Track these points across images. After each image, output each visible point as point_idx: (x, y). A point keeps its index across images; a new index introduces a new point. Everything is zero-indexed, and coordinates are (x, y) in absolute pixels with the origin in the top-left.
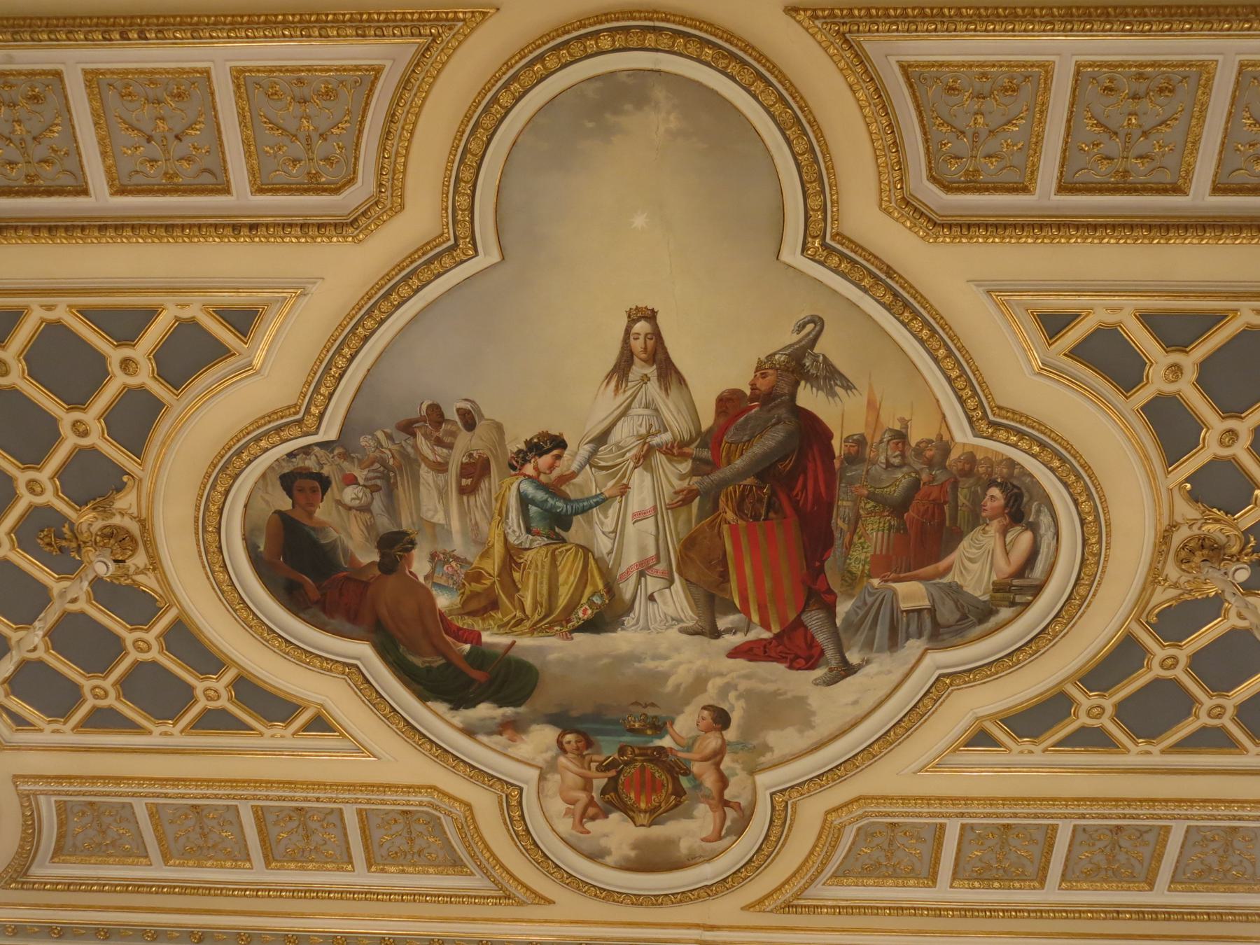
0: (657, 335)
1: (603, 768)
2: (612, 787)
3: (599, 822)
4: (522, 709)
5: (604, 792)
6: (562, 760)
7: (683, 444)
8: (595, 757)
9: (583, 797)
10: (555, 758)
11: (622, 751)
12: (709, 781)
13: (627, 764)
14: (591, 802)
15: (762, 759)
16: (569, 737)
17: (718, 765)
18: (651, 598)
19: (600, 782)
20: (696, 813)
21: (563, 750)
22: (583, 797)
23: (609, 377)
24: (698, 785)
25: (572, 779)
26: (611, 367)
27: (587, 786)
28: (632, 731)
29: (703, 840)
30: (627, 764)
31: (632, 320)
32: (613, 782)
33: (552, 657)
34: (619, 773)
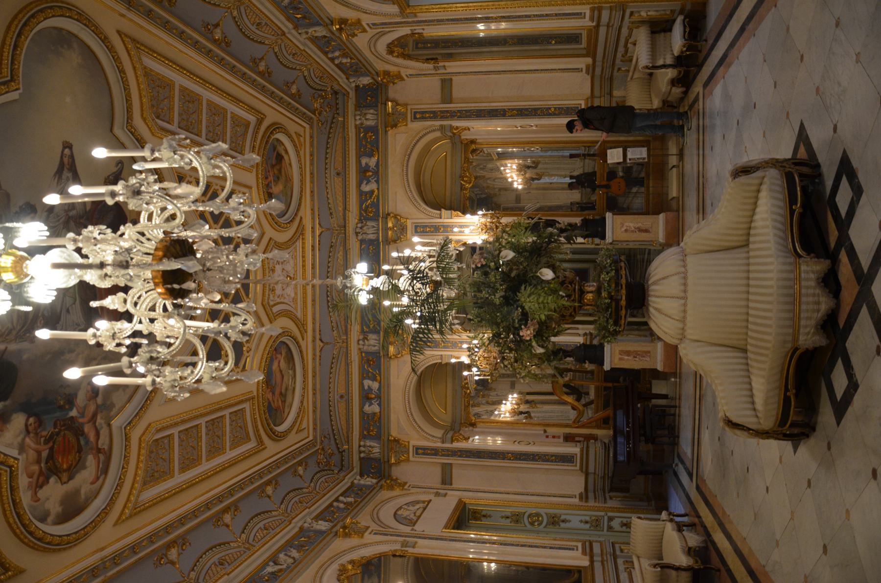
0: (72, 156)
1: (46, 442)
2: (51, 457)
3: (45, 488)
4: (8, 403)
5: (46, 463)
6: (28, 440)
7: (81, 217)
8: (44, 433)
9: (35, 468)
10: (24, 439)
11: (55, 426)
12: (92, 438)
13: (58, 434)
14: (41, 473)
15: (112, 413)
16: (31, 420)
17: (95, 423)
18: (68, 311)
19: (45, 454)
20: (88, 464)
21: (28, 432)
22: (35, 468)
23: (55, 175)
24: (87, 442)
25: (32, 454)
26: (55, 170)
27: (38, 462)
28: (61, 408)
29: (92, 483)
30: (58, 434)
31: (64, 148)
32: (51, 449)
33: (25, 357)
34: (54, 443)
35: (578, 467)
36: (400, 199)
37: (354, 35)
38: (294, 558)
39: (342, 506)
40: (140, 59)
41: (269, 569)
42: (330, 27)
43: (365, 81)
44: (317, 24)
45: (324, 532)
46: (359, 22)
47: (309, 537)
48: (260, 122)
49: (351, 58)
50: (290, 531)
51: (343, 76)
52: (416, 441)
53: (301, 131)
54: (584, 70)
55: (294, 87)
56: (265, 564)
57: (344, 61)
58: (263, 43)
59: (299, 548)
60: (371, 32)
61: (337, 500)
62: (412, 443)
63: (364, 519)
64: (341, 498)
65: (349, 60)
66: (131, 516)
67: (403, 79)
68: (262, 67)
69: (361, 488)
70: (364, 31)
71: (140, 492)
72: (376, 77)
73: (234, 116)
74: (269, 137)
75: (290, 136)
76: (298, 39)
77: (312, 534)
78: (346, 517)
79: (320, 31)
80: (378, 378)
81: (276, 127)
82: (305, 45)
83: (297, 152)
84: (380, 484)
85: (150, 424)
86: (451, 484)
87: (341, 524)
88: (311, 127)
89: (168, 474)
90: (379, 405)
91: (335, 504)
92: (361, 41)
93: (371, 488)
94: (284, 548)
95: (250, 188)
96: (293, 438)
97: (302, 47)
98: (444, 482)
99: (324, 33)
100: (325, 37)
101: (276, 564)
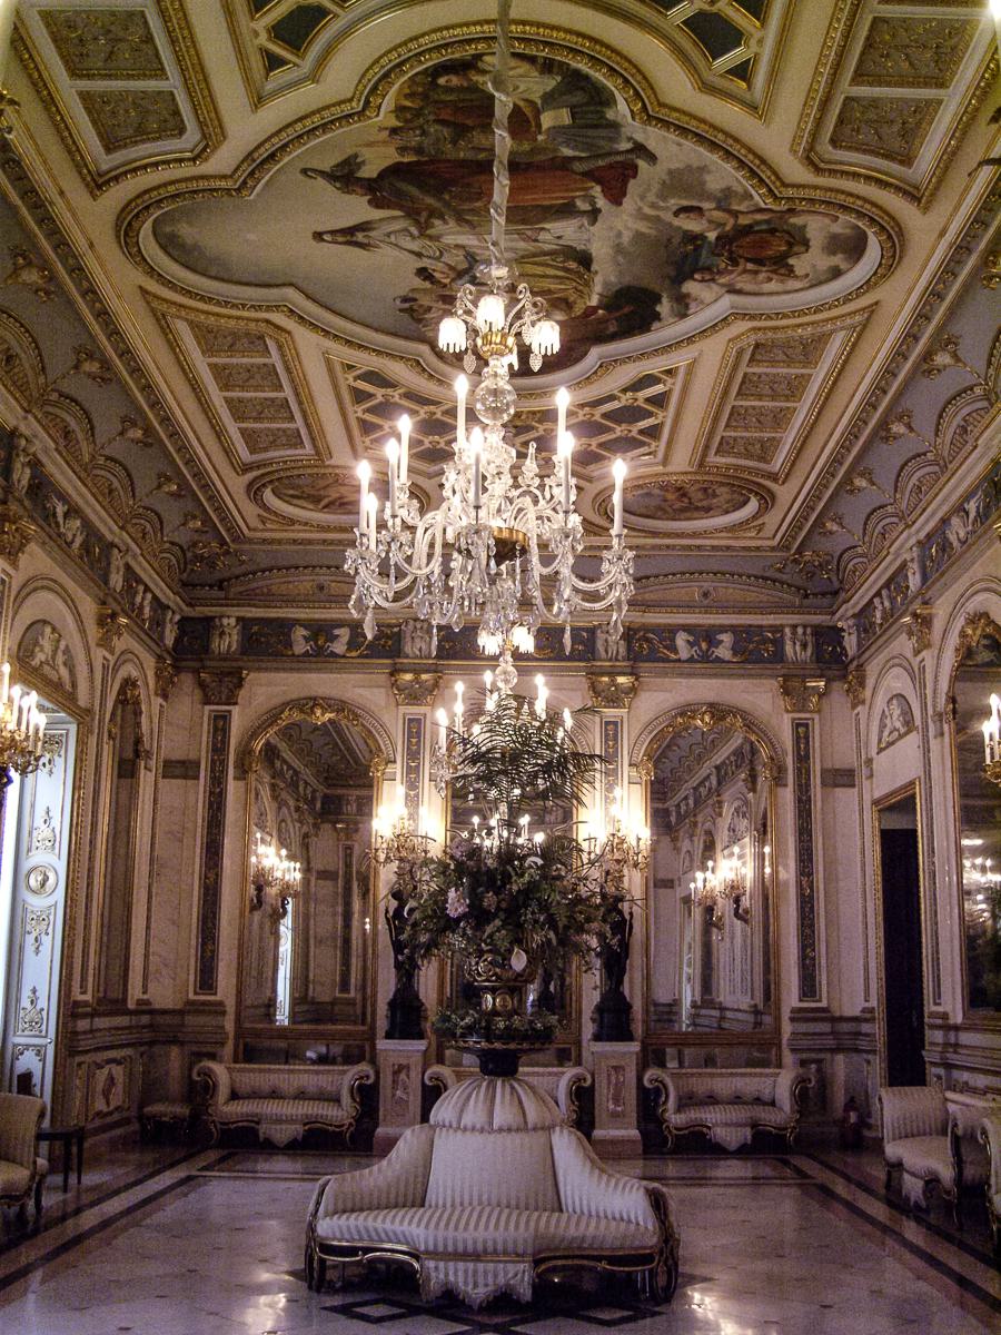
35: (191, 996)
36: (659, 698)
37: (910, 634)
38: (73, 541)
39: (138, 599)
40: (842, 329)
41: (60, 509)
42: (919, 600)
43: (850, 642)
44: (925, 578)
45: (106, 582)
46: (928, 646)
47: (99, 560)
48: (774, 477)
49: (881, 625)
50: (108, 528)
51: (857, 610)
52: (239, 720)
53: (768, 532)
54: (867, 1005)
55: (835, 528)
56: (63, 498)
57: (878, 614)
58: (896, 491)
59: (86, 547)
60: (915, 662)
61: (147, 589)
62: (235, 710)
63: (124, 642)
64: (149, 596)
65: (879, 621)
66: (154, 312)
67: (854, 707)
68: (860, 482)
69: (158, 623)
70: (917, 652)
71: (187, 320)
72: (855, 663)
73: (775, 443)
74: (751, 491)
75: (755, 517)
76: (905, 546)
77: (104, 564)
78: (129, 617)
79: (914, 581)
80: (354, 654)
81: (768, 500)
82: (897, 555)
83: (726, 529)
84: (166, 656)
85: (289, 333)
86: (164, 777)
87: (118, 609)
88: (773, 549)
89: (208, 350)
90: (306, 654)
91: (141, 588)
92: (903, 644)
93: (159, 641)
94: (87, 525)
95: (665, 462)
96: (251, 510)
97: (892, 550)
98: (168, 764)
99: (912, 587)
100: (908, 587)
101: (66, 515)
